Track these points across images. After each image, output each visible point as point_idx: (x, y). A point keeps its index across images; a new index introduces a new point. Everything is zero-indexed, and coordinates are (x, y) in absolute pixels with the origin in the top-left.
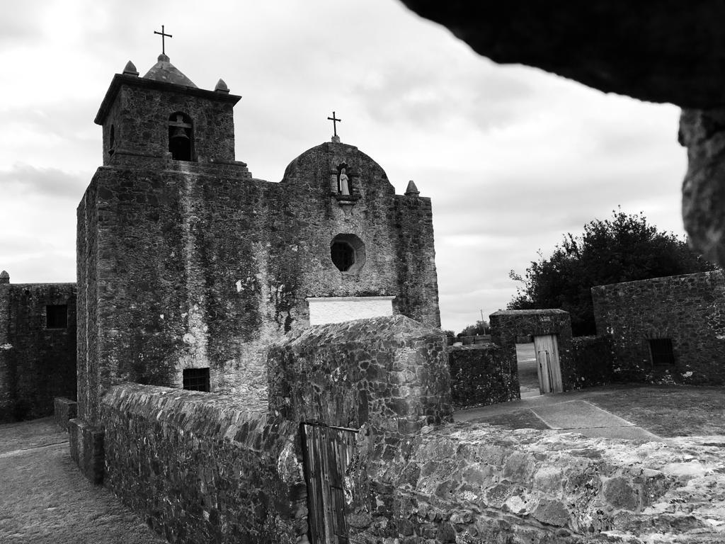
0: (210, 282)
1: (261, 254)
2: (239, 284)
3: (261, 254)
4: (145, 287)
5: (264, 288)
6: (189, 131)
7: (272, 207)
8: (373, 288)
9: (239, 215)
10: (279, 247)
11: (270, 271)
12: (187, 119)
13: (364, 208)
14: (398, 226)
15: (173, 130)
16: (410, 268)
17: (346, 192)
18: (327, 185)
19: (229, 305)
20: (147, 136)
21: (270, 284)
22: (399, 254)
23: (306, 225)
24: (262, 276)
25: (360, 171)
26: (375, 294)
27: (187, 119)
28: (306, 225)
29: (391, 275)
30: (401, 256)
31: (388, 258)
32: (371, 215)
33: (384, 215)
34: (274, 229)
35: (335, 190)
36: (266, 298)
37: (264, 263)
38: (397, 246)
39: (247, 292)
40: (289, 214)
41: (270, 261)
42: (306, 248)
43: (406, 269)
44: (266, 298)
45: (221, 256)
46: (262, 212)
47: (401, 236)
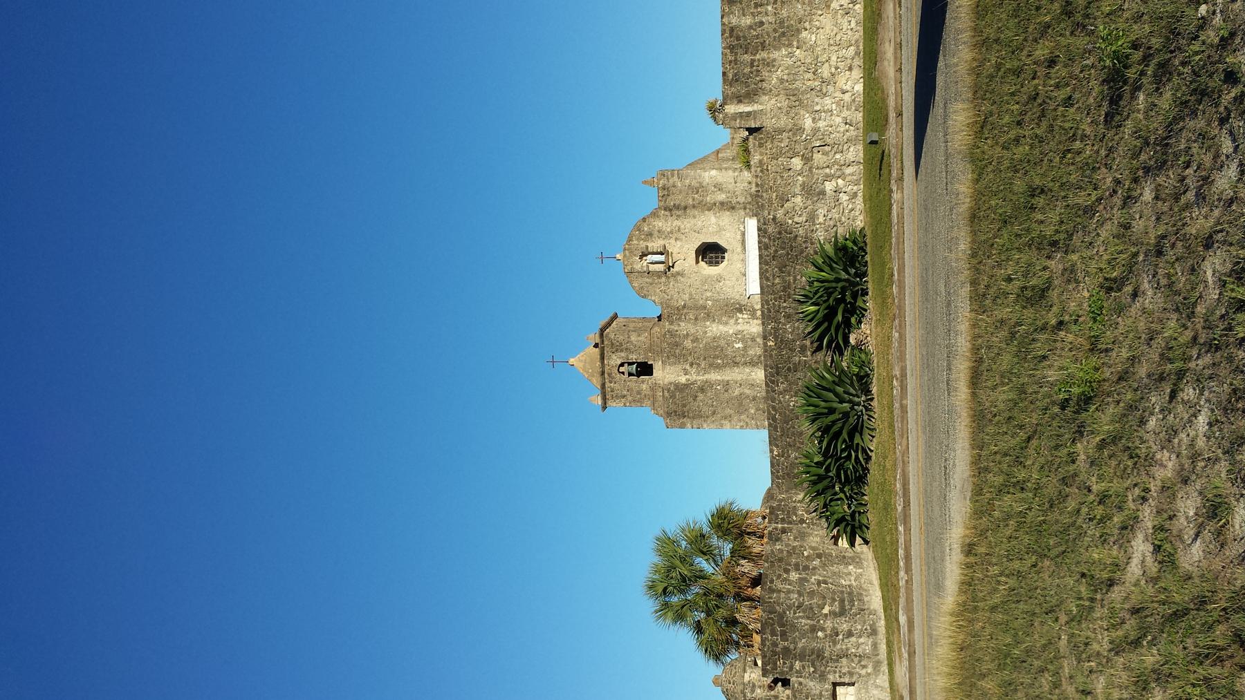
0: (736, 364)
1: (715, 329)
2: (737, 346)
3: (715, 329)
4: (741, 404)
5: (739, 328)
6: (630, 364)
7: (680, 319)
8: (739, 237)
9: (688, 344)
10: (708, 316)
11: (726, 323)
12: (622, 365)
13: (672, 241)
14: (685, 208)
15: (630, 374)
16: (722, 197)
17: (662, 258)
18: (658, 274)
19: (751, 352)
20: (639, 393)
21: (736, 323)
22: (709, 210)
23: (691, 294)
24: (730, 329)
25: (643, 244)
26: (743, 234)
27: (622, 365)
28: (691, 294)
29: (726, 218)
30: (710, 207)
31: (713, 219)
32: (676, 233)
33: (677, 223)
34: (696, 319)
35: (661, 267)
36: (746, 327)
37: (721, 327)
38: (703, 211)
39: (743, 340)
40: (684, 307)
41: (720, 322)
42: (709, 294)
43: (722, 204)
44: (746, 327)
45: (716, 357)
46: (684, 327)
47: (694, 207)
